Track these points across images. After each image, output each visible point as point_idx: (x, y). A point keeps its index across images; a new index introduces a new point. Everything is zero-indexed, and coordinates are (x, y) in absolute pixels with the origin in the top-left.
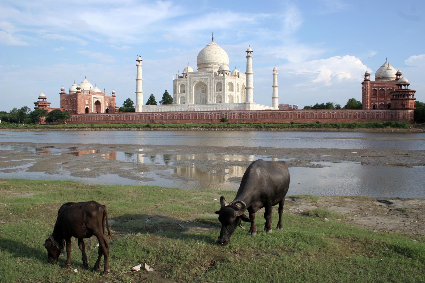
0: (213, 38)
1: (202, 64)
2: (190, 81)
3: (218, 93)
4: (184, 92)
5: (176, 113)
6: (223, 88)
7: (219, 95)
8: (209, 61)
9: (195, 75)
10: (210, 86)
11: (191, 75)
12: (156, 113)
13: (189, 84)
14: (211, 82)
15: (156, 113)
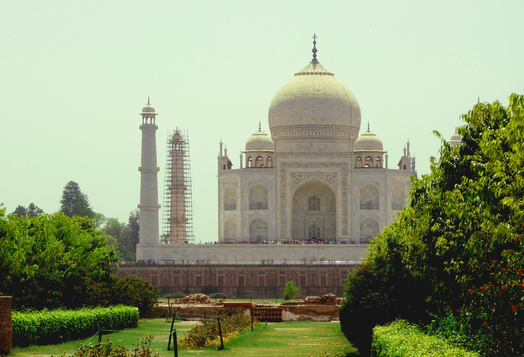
0: (315, 51)
1: (300, 126)
2: (283, 177)
3: (366, 213)
4: (260, 206)
5: (285, 269)
6: (381, 200)
7: (368, 219)
8: (323, 119)
9: (299, 160)
10: (344, 194)
11: (286, 160)
12: (221, 269)
13: (279, 186)
14: (344, 183)
15: (221, 269)
